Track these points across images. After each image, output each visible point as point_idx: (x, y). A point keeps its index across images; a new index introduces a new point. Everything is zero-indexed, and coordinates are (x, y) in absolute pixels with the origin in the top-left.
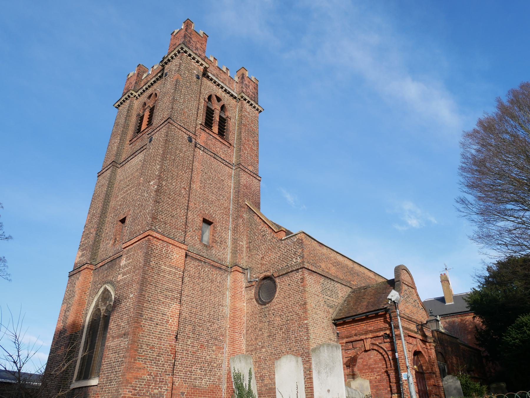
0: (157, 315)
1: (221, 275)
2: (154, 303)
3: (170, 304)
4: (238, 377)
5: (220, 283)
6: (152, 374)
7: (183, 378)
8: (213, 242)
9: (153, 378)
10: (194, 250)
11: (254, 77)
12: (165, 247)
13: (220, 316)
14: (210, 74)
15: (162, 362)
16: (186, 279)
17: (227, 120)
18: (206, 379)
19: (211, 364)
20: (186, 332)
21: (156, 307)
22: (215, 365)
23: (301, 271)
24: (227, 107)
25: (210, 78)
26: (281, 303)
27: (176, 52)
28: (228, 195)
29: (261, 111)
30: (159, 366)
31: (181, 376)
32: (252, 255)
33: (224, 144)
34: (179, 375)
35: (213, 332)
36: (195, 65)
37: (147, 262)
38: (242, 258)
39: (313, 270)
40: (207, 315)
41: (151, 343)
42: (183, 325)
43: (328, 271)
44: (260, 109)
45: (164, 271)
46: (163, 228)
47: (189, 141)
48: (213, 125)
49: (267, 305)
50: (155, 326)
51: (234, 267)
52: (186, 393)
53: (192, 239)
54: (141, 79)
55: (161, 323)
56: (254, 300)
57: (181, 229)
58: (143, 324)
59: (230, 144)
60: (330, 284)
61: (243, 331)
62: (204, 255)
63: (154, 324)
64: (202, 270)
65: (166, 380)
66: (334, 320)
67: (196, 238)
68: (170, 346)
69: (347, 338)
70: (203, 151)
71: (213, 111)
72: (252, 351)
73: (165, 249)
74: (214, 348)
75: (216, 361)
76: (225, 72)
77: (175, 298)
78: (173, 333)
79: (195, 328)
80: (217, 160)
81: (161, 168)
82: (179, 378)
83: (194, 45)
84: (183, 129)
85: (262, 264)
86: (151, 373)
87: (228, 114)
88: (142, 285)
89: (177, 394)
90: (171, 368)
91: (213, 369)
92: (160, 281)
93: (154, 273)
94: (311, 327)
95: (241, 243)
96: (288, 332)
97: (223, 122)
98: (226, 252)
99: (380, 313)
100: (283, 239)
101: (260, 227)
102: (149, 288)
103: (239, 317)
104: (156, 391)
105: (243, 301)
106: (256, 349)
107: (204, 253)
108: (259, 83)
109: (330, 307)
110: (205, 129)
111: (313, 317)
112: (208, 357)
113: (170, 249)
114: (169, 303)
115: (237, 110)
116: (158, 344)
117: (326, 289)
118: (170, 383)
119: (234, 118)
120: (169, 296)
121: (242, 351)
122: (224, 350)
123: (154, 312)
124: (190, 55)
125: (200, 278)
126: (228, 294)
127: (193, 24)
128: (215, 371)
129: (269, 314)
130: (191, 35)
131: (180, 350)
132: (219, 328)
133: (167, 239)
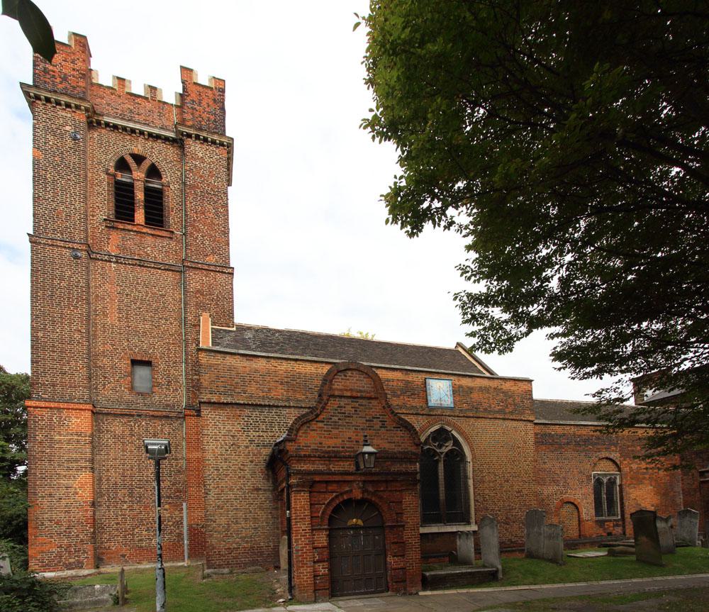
39: (222, 401)
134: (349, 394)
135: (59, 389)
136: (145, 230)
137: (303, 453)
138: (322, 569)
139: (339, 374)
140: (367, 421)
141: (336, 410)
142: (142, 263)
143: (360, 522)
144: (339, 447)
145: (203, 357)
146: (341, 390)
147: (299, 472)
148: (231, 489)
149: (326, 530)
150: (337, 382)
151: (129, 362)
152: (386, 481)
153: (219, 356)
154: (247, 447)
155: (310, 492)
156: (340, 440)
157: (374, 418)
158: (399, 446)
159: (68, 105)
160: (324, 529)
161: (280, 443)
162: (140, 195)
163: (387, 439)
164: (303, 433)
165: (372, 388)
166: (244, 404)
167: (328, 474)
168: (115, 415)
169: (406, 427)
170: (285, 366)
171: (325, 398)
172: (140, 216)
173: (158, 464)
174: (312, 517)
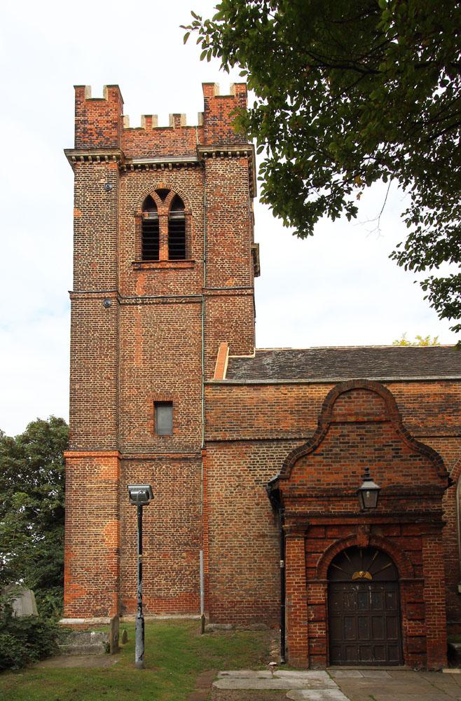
134: (353, 419)
136: (168, 265)
137: (297, 493)
138: (319, 631)
139: (342, 396)
140: (375, 450)
141: (337, 439)
142: (164, 301)
143: (368, 576)
144: (339, 484)
145: (209, 393)
146: (343, 415)
147: (293, 515)
148: (236, 536)
149: (324, 583)
150: (338, 406)
151: (152, 404)
152: (400, 525)
153: (225, 389)
154: (253, 488)
155: (306, 539)
156: (342, 475)
157: (384, 446)
158: (418, 479)
159: (102, 159)
160: (321, 582)
161: (274, 482)
162: (164, 231)
163: (401, 471)
164: (299, 469)
165: (383, 408)
166: (250, 440)
167: (327, 516)
168: (139, 460)
169: (427, 455)
170: (296, 392)
171: (324, 426)
172: (164, 252)
173: (140, 510)
174: (306, 568)
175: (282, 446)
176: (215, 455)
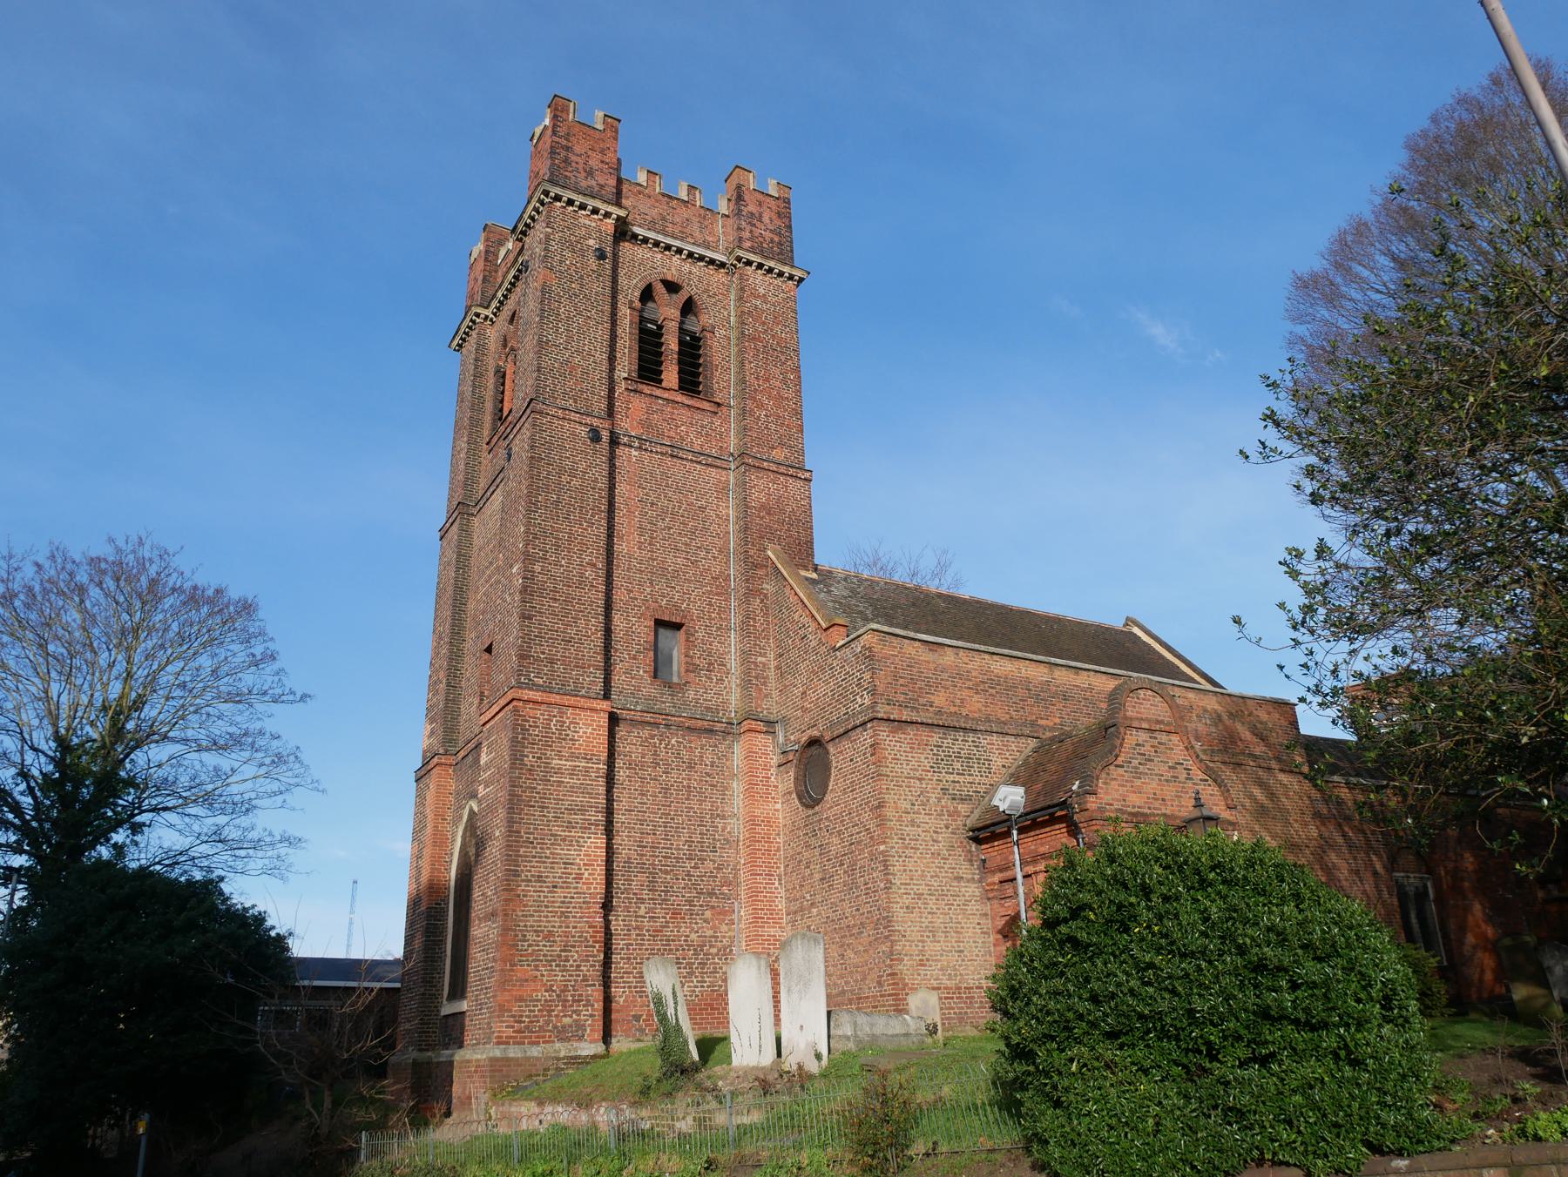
0: (553, 868)
1: (716, 746)
2: (543, 844)
3: (582, 840)
4: (659, 1001)
5: (712, 766)
6: (554, 988)
7: (636, 987)
8: (687, 671)
9: (558, 996)
10: (637, 702)
11: (775, 182)
12: (555, 716)
13: (719, 840)
14: (637, 230)
15: (575, 961)
16: (621, 773)
17: (705, 337)
18: (692, 982)
19: (702, 950)
20: (632, 889)
21: (548, 852)
22: (714, 951)
23: (871, 728)
24: (702, 300)
25: (640, 237)
26: (839, 804)
27: (534, 203)
28: (720, 543)
29: (801, 280)
30: (568, 971)
31: (628, 982)
32: (786, 687)
33: (698, 408)
34: (624, 982)
35: (702, 881)
36: (588, 223)
37: (517, 759)
38: (766, 696)
39: (904, 718)
40: (684, 845)
41: (545, 927)
42: (623, 875)
43: (957, 708)
44: (798, 274)
45: (559, 771)
46: (546, 674)
47: (592, 440)
48: (663, 368)
49: (817, 808)
50: (550, 892)
51: (745, 723)
52: (644, 1017)
53: (632, 676)
54: (496, 265)
55: (565, 882)
56: (794, 795)
57: (594, 665)
58: (523, 890)
59: (719, 405)
60: (961, 744)
61: (778, 868)
62: (668, 708)
63: (548, 887)
64: (663, 745)
65: (588, 995)
66: (973, 831)
67: (641, 673)
68: (589, 927)
69: (1001, 871)
70: (640, 448)
71: (660, 327)
72: (796, 912)
73: (557, 721)
74: (708, 914)
75: (716, 941)
76: (686, 199)
77: (592, 824)
78: (596, 898)
79: (654, 878)
80: (682, 458)
81: (527, 532)
82: (624, 987)
83: (580, 167)
84: (573, 414)
85: (804, 710)
86: (552, 986)
87: (706, 319)
88: (511, 810)
89: (623, 1020)
90: (598, 971)
91: (708, 959)
92: (550, 794)
93: (535, 779)
94: (897, 858)
95: (760, 659)
96: (853, 870)
97: (691, 349)
98: (725, 688)
99: (1059, 814)
100: (838, 645)
101: (796, 617)
102: (527, 814)
103: (763, 838)
104: (567, 1020)
105: (773, 798)
106: (802, 909)
107: (664, 703)
108: (792, 196)
109: (962, 799)
110: (641, 387)
111: (902, 834)
112: (693, 936)
113: (568, 718)
114: (579, 837)
115: (732, 297)
116: (560, 927)
117: (951, 756)
118: (597, 1001)
119: (724, 326)
120: (577, 823)
121: (777, 914)
122: (735, 916)
123: (544, 862)
124: (570, 202)
125: (659, 764)
126: (737, 787)
127: (572, 105)
128: (715, 963)
129: (820, 829)
130: (568, 140)
131: (622, 930)
132: (718, 869)
133: (558, 697)
135: (559, 666)
175: (970, 739)
176: (887, 742)
